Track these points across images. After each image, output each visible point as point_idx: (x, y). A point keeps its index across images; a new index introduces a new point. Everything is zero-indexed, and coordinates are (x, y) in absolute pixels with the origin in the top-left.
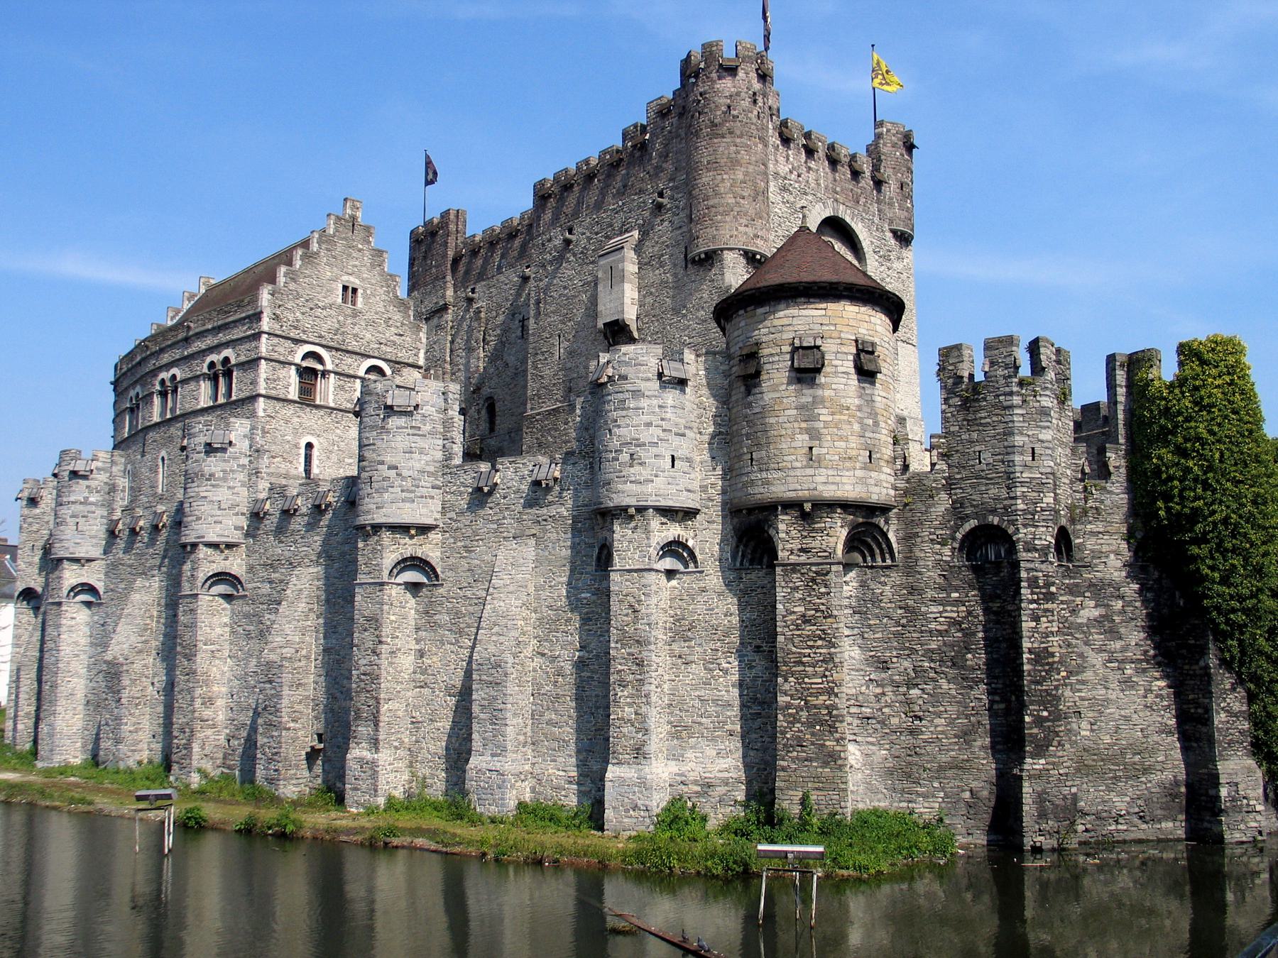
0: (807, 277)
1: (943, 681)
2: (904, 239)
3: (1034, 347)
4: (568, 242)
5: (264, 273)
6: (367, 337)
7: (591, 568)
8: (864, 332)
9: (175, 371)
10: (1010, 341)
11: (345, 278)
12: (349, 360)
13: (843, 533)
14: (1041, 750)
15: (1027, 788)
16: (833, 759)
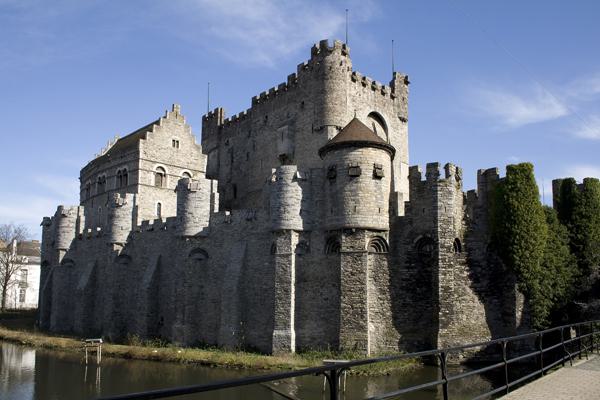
0: (355, 139)
1: (408, 300)
2: (403, 120)
3: (447, 167)
4: (265, 122)
5: (141, 134)
6: (183, 161)
7: (268, 253)
8: (378, 161)
9: (104, 174)
10: (435, 165)
11: (174, 137)
12: (175, 169)
13: (368, 240)
14: (445, 326)
15: (439, 340)
16: (363, 329)
